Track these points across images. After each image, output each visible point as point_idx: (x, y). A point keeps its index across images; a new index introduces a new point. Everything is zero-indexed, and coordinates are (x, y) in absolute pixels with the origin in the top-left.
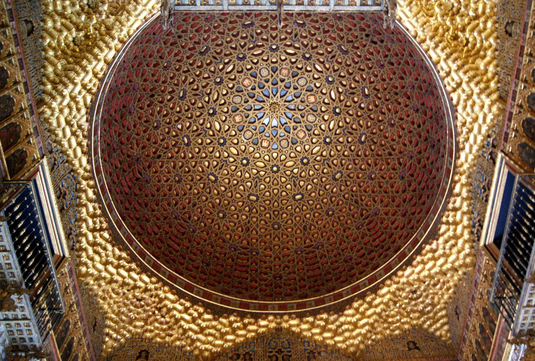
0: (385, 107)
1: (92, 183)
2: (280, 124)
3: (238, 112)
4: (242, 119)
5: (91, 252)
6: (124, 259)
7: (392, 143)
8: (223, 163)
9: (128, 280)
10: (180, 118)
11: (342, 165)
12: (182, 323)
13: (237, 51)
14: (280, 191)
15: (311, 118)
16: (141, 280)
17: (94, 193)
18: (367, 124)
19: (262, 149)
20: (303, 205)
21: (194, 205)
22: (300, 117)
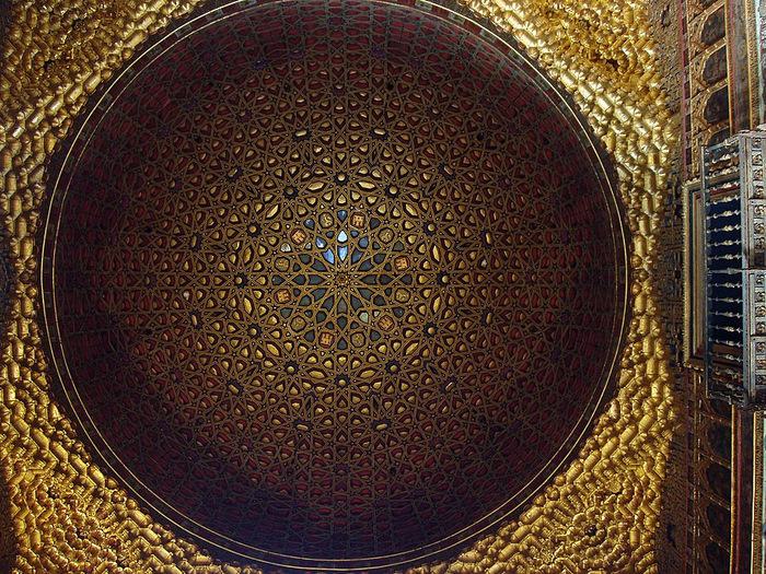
0: (518, 255)
1: (34, 291)
2: (350, 308)
3: (282, 285)
4: (290, 297)
5: (12, 396)
6: (67, 430)
7: (535, 310)
8: (254, 368)
9: (65, 465)
10: (188, 281)
11: (456, 367)
12: (154, 559)
13: (284, 182)
14: (350, 416)
15: (402, 295)
16: (90, 474)
17: (35, 308)
18: (493, 292)
19: (321, 349)
20: (391, 438)
21: (199, 422)
22: (383, 295)
